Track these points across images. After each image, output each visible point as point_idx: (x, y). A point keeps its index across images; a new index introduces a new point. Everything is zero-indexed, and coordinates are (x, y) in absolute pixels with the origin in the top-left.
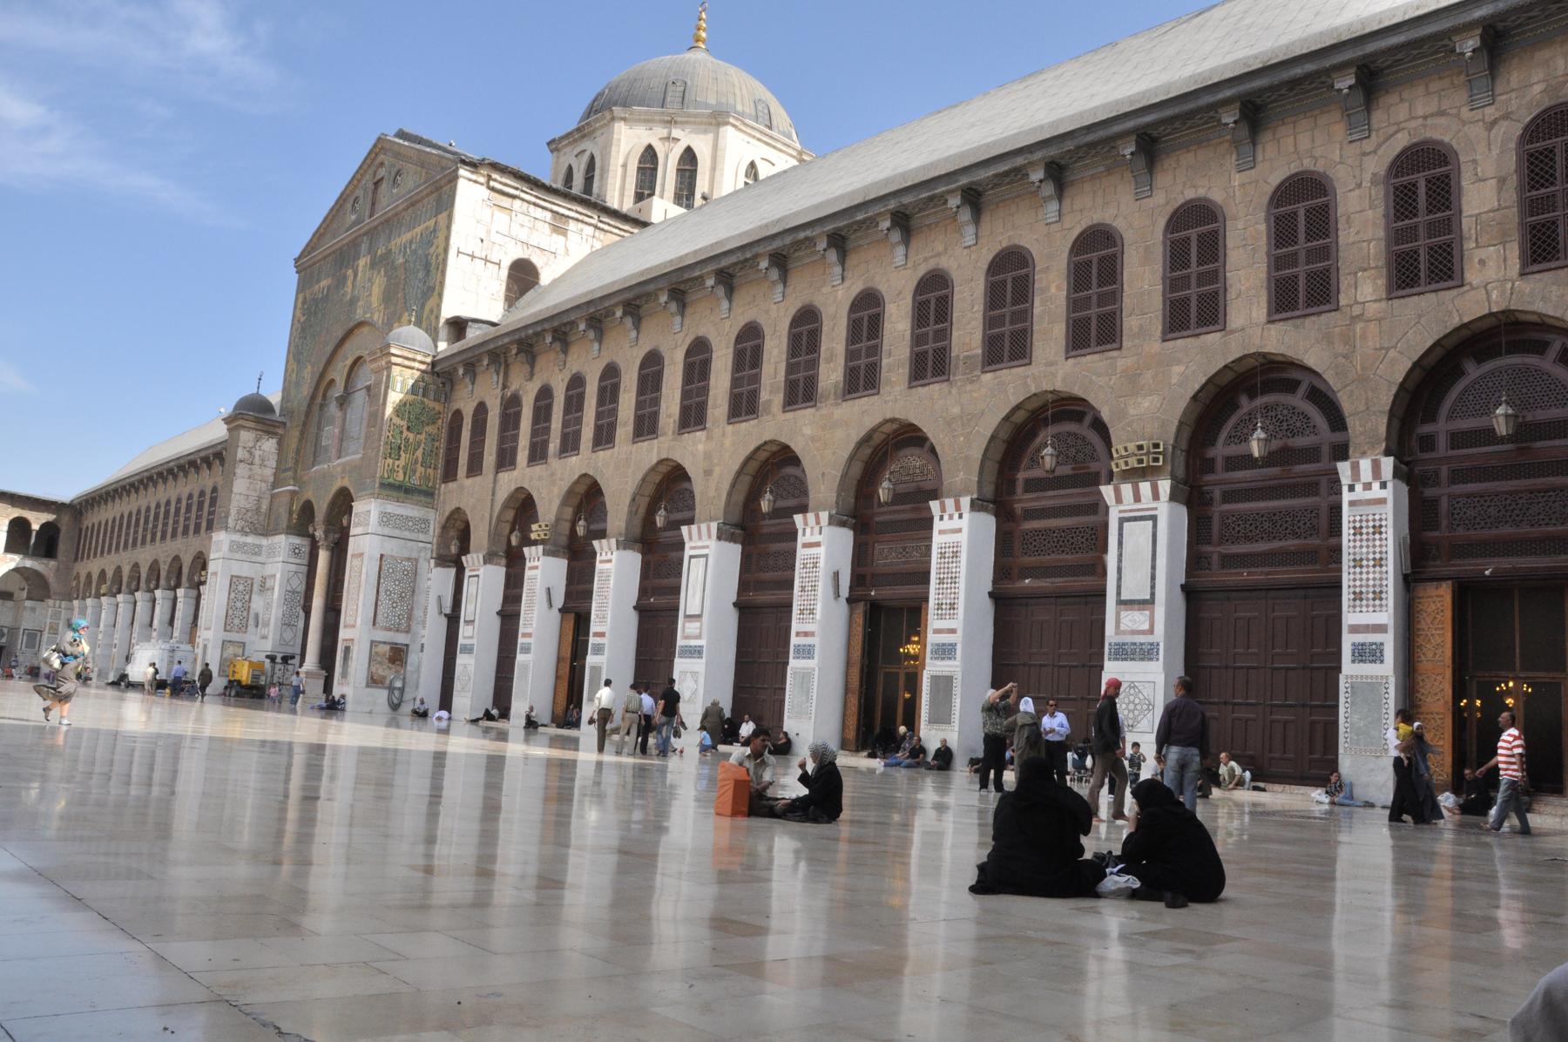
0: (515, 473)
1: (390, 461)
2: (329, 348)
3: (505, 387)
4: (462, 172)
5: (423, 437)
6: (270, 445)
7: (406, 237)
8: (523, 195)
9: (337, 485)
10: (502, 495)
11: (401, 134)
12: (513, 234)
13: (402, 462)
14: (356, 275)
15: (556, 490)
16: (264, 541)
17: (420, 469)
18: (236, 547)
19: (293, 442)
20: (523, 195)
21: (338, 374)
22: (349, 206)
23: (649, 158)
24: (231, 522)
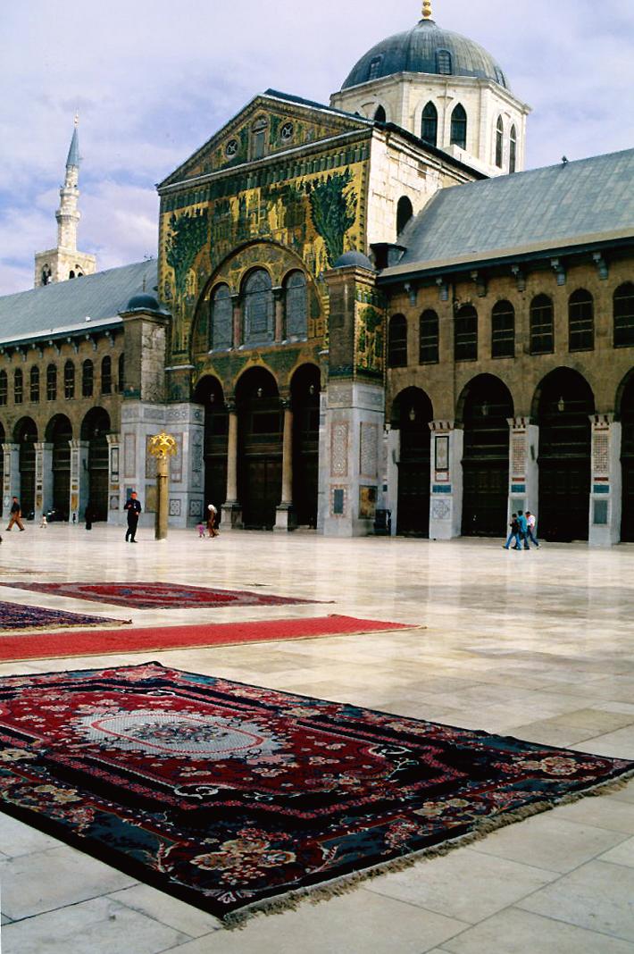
0: (478, 363)
1: (360, 353)
2: (217, 260)
3: (454, 300)
4: (374, 133)
5: (375, 334)
6: (160, 333)
7: (313, 177)
8: (406, 150)
9: (250, 364)
10: (464, 380)
11: (269, 92)
12: (400, 179)
13: (365, 354)
14: (243, 202)
15: (530, 377)
16: (164, 408)
17: (375, 358)
18: (148, 414)
19: (184, 328)
20: (406, 150)
21: (232, 278)
22: (222, 147)
23: (430, 113)
24: (142, 393)
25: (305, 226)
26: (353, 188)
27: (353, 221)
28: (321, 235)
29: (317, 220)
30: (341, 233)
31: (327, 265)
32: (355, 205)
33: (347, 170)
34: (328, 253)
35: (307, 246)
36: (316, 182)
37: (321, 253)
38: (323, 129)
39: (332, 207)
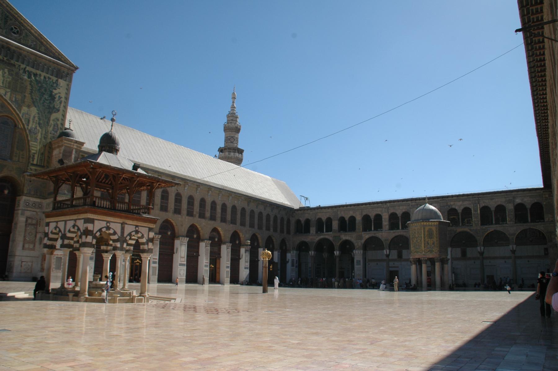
7: (34, 71)
25: (25, 96)
26: (60, 93)
27: (58, 111)
28: (36, 107)
29: (34, 97)
30: (50, 113)
31: (38, 125)
32: (61, 103)
33: (57, 80)
34: (40, 119)
35: (25, 109)
36: (35, 75)
37: (34, 117)
38: (43, 48)
39: (46, 96)
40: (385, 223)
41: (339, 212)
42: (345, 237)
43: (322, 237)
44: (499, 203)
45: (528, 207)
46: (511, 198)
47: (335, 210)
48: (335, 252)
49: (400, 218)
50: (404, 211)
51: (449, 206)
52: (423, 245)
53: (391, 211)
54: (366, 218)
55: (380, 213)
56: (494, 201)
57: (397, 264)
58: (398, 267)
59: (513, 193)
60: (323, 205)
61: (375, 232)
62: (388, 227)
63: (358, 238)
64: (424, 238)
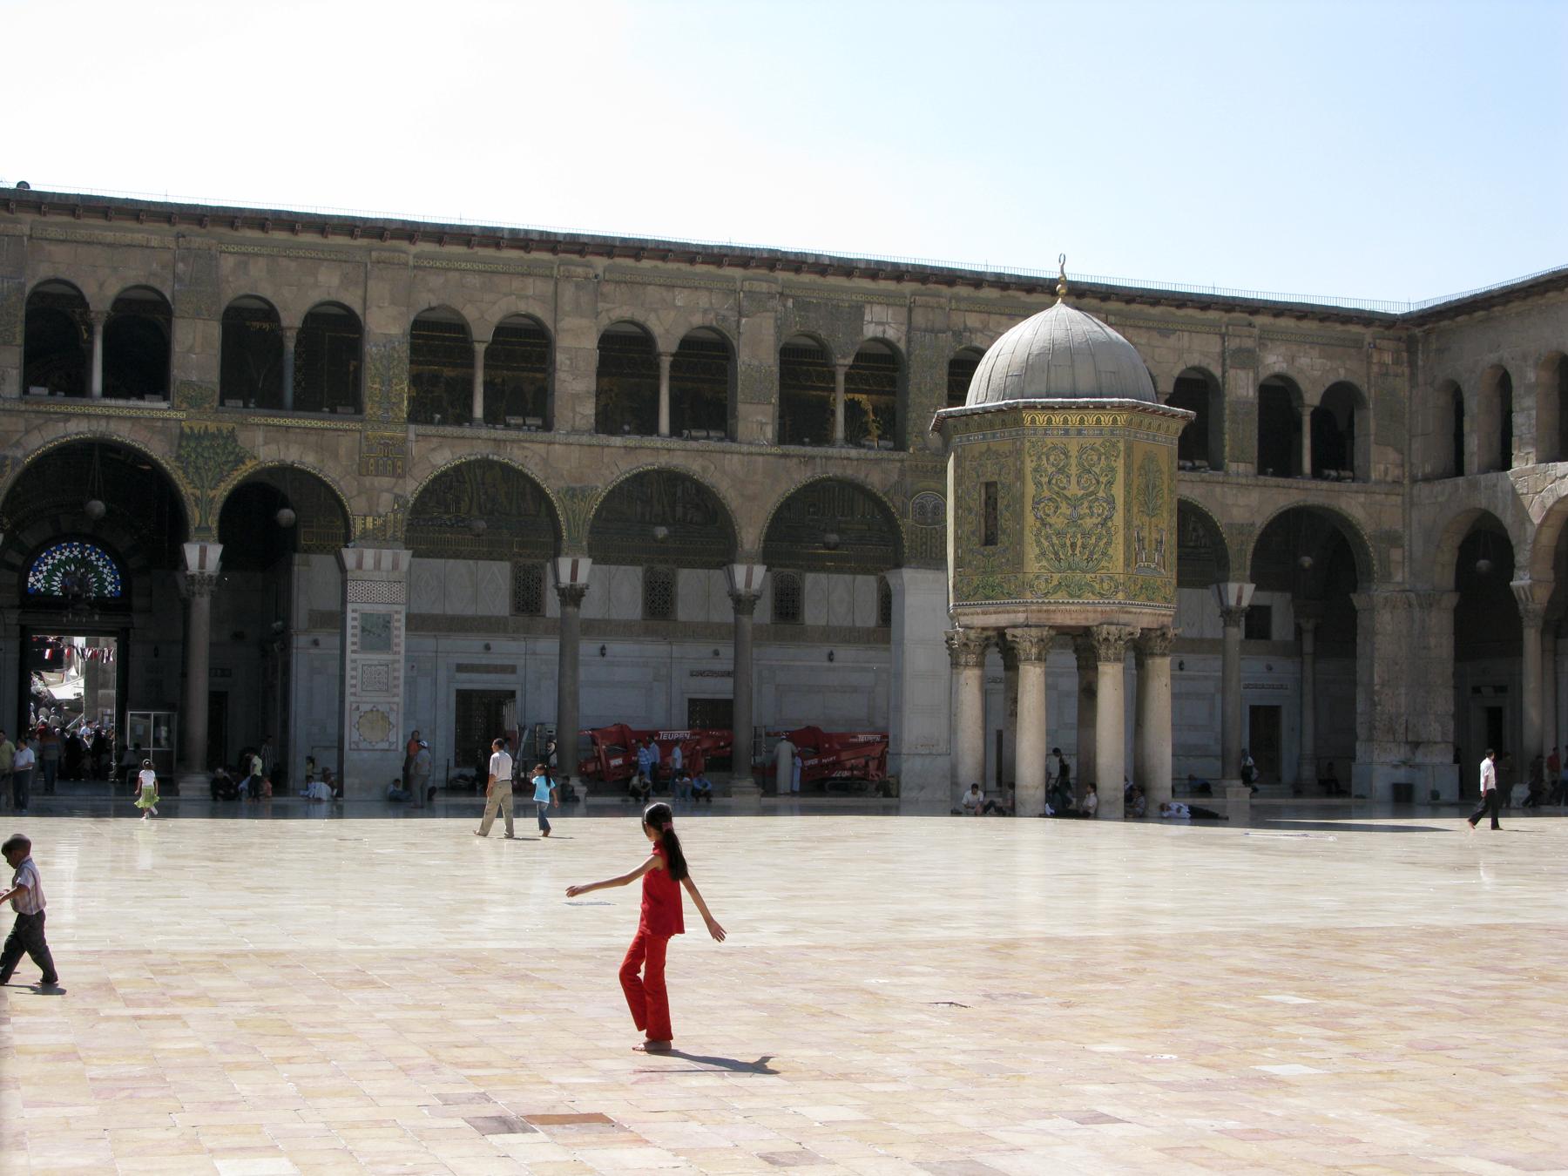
40: (575, 378)
41: (227, 263)
42: (274, 442)
43: (77, 429)
44: (1195, 360)
45: (1312, 397)
46: (1249, 343)
47: (199, 239)
48: (192, 553)
49: (666, 363)
50: (697, 320)
51: (958, 335)
52: (1118, 551)
53: (619, 309)
54: (437, 338)
55: (538, 311)
56: (1172, 341)
57: (506, 648)
58: (512, 669)
59: (1260, 320)
60: (44, 181)
61: (499, 433)
62: (589, 409)
63: (373, 458)
64: (1128, 510)
